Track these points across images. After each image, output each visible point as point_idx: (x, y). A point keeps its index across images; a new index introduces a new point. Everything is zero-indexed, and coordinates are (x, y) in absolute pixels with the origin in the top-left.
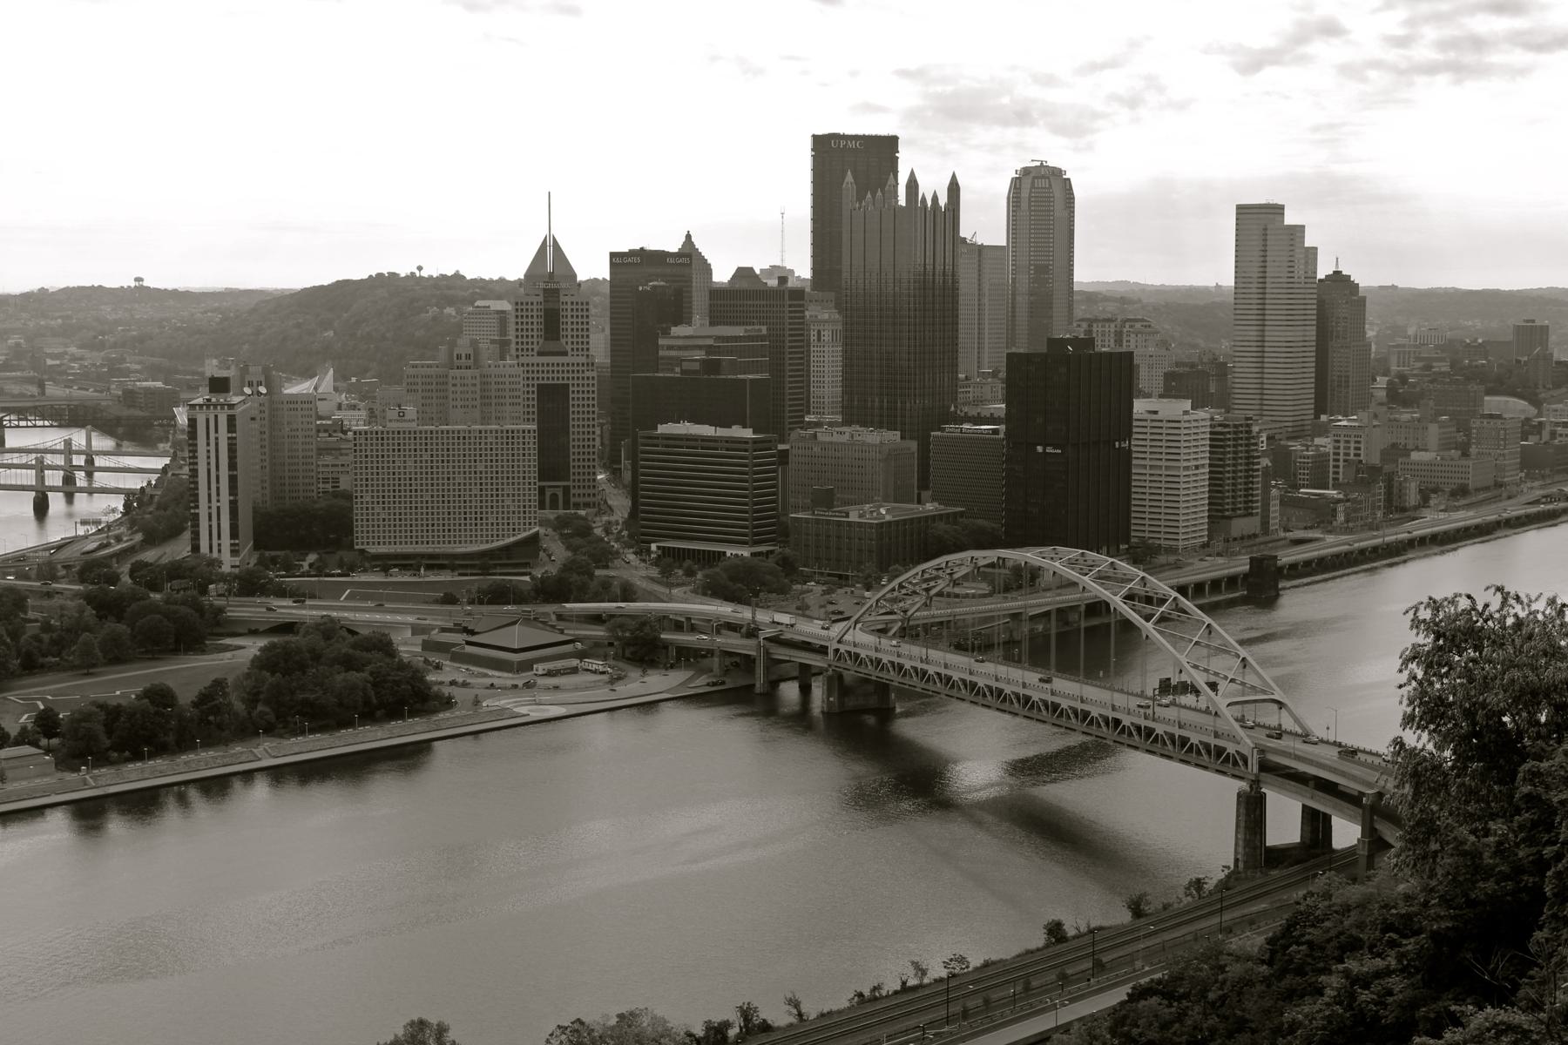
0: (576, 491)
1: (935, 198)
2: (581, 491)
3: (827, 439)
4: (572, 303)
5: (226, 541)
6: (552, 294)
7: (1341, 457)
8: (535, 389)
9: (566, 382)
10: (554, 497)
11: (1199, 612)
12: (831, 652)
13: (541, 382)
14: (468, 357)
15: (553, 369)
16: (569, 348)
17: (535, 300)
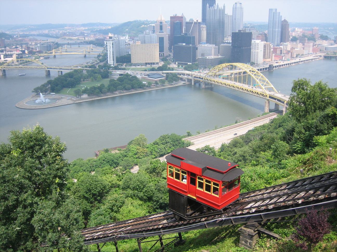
0: (165, 54)
1: (221, 8)
2: (166, 54)
3: (204, 46)
5: (112, 62)
7: (284, 49)
10: (162, 55)
11: (261, 73)
14: (148, 33)
15: (162, 35)
17: (158, 24)
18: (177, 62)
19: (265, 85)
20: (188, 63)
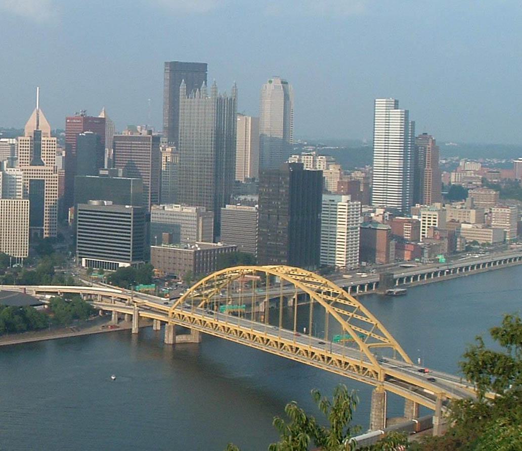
3: (170, 210)
4: (47, 141)
6: (37, 135)
8: (28, 182)
9: (43, 179)
10: (36, 234)
12: (170, 315)
13: (31, 178)
15: (37, 172)
16: (45, 162)
17: (29, 138)
18: (84, 259)
19: (372, 340)
20: (121, 265)
